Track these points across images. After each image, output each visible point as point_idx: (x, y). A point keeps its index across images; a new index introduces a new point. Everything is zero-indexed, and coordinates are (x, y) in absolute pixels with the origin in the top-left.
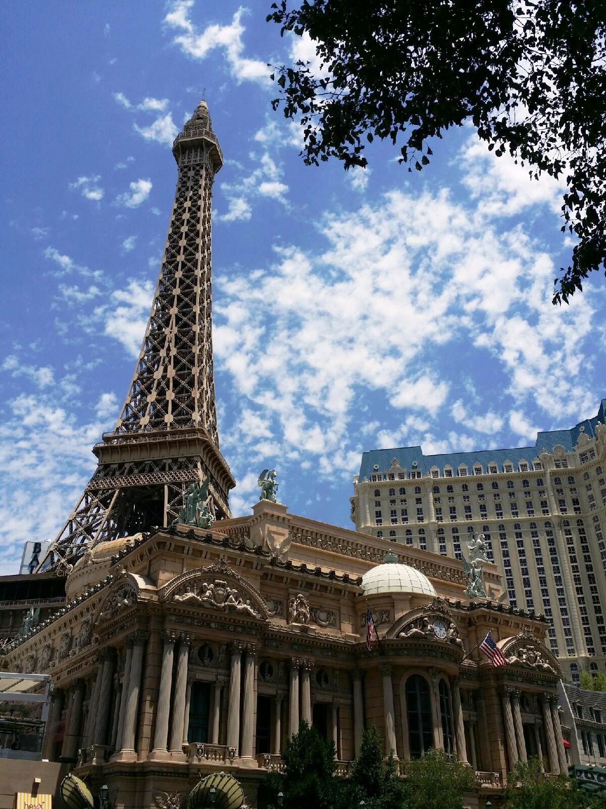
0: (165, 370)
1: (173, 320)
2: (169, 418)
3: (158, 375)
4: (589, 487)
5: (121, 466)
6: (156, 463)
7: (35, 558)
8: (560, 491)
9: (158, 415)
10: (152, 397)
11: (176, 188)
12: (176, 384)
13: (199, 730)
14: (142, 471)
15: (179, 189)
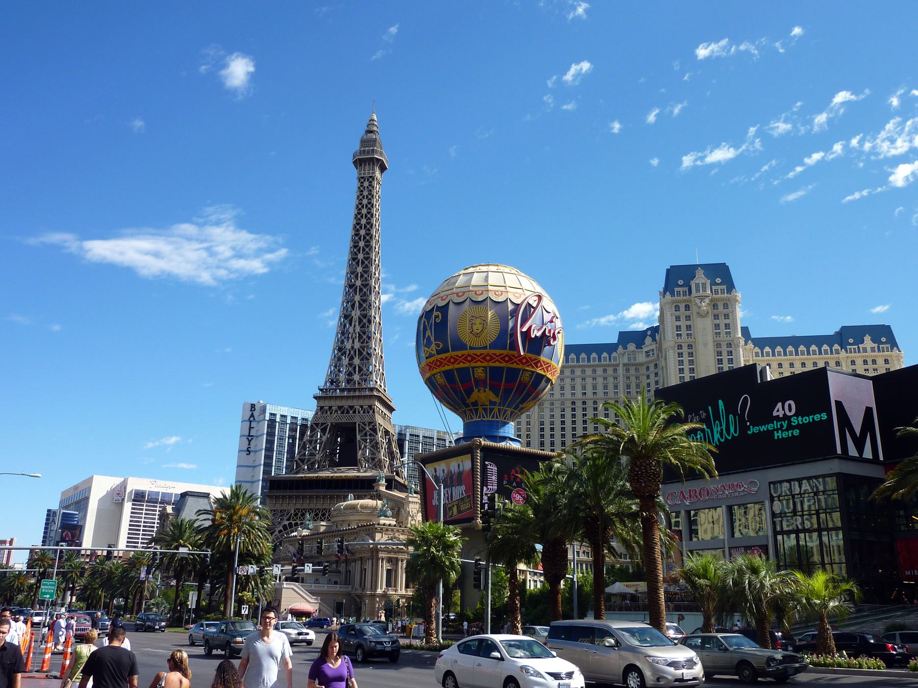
0: (353, 342)
1: (357, 304)
2: (356, 377)
3: (348, 345)
4: (648, 377)
5: (330, 408)
6: (351, 407)
7: (252, 415)
8: (628, 378)
9: (350, 374)
10: (345, 361)
11: (356, 197)
12: (360, 353)
13: (389, 584)
14: (342, 413)
15: (357, 206)
